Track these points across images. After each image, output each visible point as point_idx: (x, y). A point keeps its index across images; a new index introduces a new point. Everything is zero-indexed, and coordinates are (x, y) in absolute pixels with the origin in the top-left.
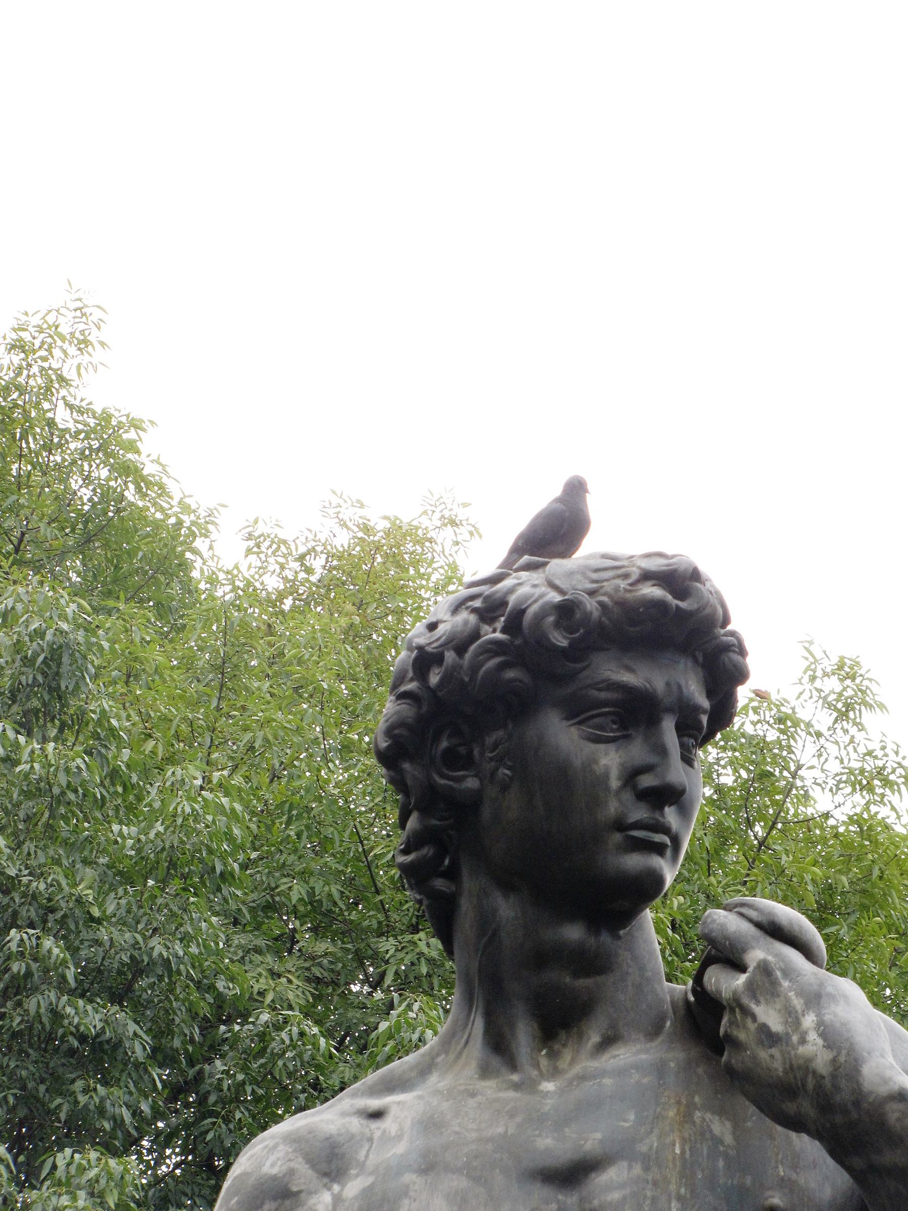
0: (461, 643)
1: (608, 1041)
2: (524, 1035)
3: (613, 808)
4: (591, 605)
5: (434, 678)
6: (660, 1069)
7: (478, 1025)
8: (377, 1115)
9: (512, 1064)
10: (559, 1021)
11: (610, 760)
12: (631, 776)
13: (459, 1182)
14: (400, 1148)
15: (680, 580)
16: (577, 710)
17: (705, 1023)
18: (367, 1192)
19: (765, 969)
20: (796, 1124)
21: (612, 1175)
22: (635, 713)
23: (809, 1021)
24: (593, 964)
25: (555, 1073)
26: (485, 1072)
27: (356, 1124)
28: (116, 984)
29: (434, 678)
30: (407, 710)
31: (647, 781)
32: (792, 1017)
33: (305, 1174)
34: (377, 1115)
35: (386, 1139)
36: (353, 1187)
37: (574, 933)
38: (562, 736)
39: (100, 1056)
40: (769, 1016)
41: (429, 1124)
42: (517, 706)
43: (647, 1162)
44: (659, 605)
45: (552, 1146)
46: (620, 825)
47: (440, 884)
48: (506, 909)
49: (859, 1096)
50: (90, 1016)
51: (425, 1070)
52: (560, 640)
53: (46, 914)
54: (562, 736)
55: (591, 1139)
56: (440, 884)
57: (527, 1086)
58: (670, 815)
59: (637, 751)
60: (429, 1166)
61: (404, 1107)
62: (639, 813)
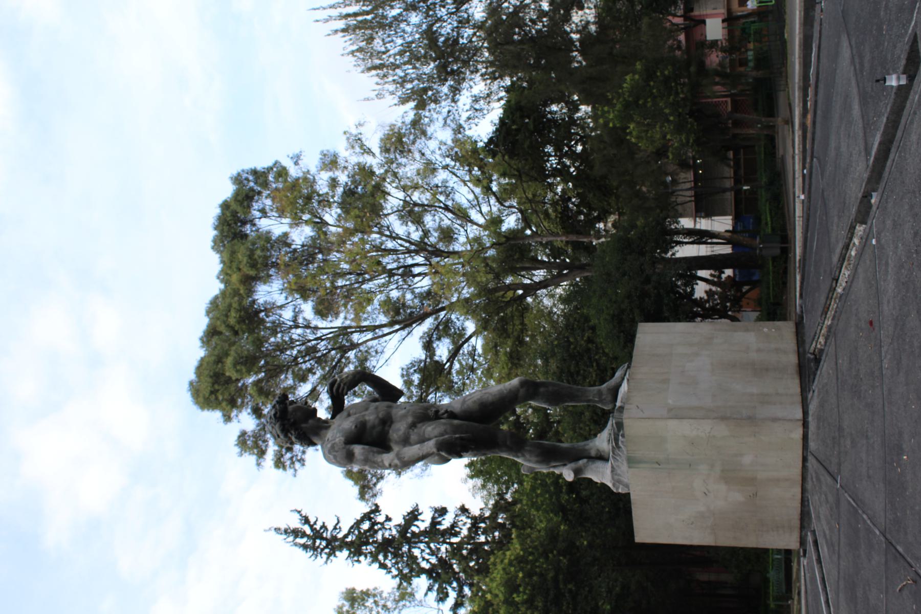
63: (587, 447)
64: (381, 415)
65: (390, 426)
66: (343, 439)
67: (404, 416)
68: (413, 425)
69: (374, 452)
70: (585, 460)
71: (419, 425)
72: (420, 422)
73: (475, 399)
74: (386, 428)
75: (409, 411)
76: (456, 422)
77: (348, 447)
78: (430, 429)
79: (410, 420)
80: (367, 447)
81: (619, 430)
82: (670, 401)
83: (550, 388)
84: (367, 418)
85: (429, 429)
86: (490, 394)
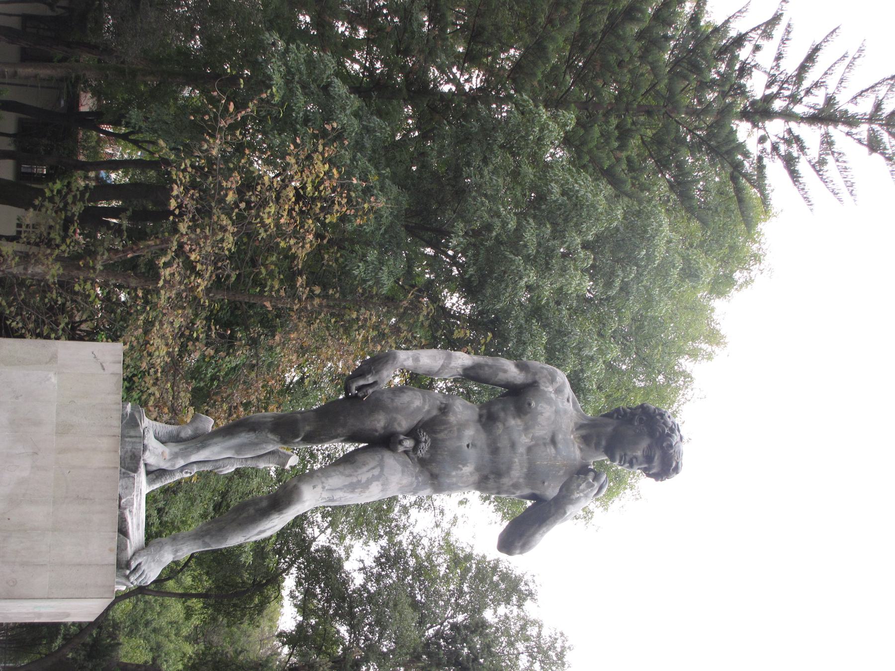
0: (665, 423)
1: (581, 449)
2: (583, 432)
3: (629, 453)
4: (672, 451)
5: (658, 417)
6: (575, 460)
7: (585, 422)
8: (568, 400)
9: (577, 429)
10: (586, 440)
11: (639, 453)
12: (636, 458)
13: (553, 418)
14: (561, 406)
15: (676, 470)
16: (650, 447)
17: (583, 471)
18: (551, 398)
19: (593, 486)
20: (561, 490)
21: (553, 451)
22: (649, 459)
23: (582, 495)
24: (597, 446)
25: (575, 438)
26: (576, 424)
27: (567, 396)
28: (625, 288)
29: (658, 417)
30: (652, 411)
31: (634, 461)
32: (583, 491)
33: (556, 385)
34: (568, 400)
35: (563, 403)
36: (553, 396)
37: (604, 443)
38: (645, 443)
39: (609, 285)
40: (583, 486)
41: (565, 412)
42: (651, 434)
43: (555, 457)
44: (671, 466)
45: (560, 437)
46: (625, 455)
47: (615, 415)
48: (610, 429)
49: (566, 504)
50: (617, 283)
51: (577, 410)
52: (665, 445)
53: (639, 275)
54: (645, 443)
55: (560, 446)
56: (615, 415)
57: (572, 432)
58: (627, 465)
59: (641, 459)
60: (557, 412)
61: (570, 407)
62: (628, 459)
63: (182, 447)
64: (500, 426)
65: (481, 416)
66: (542, 388)
67: (462, 426)
68: (444, 410)
69: (487, 365)
70: (183, 435)
71: (435, 412)
72: (436, 416)
73: (365, 469)
74: (484, 411)
75: (459, 438)
76: (379, 422)
77: (530, 380)
78: (417, 404)
79: (452, 419)
80: (501, 376)
81: (132, 415)
82: (54, 380)
83: (252, 511)
84: (519, 422)
85: (417, 403)
86: (342, 474)
